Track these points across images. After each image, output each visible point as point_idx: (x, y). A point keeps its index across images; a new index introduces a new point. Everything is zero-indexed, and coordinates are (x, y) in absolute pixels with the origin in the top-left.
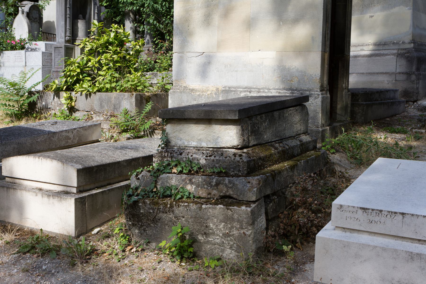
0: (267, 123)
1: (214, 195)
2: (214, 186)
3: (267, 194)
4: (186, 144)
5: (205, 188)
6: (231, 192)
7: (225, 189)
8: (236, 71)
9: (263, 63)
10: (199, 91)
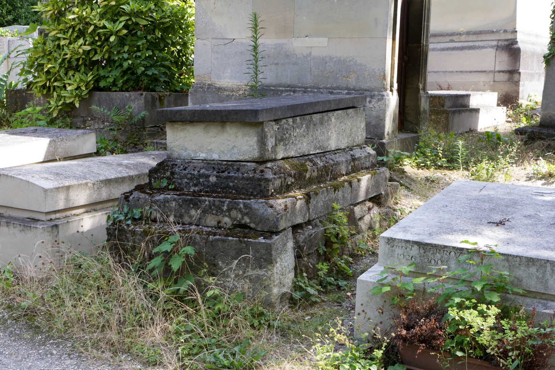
0: (303, 129)
1: (225, 223)
2: (225, 212)
3: (297, 223)
4: (192, 155)
5: (213, 214)
6: (247, 220)
7: (240, 216)
8: (276, 64)
9: (311, 53)
10: (227, 90)
